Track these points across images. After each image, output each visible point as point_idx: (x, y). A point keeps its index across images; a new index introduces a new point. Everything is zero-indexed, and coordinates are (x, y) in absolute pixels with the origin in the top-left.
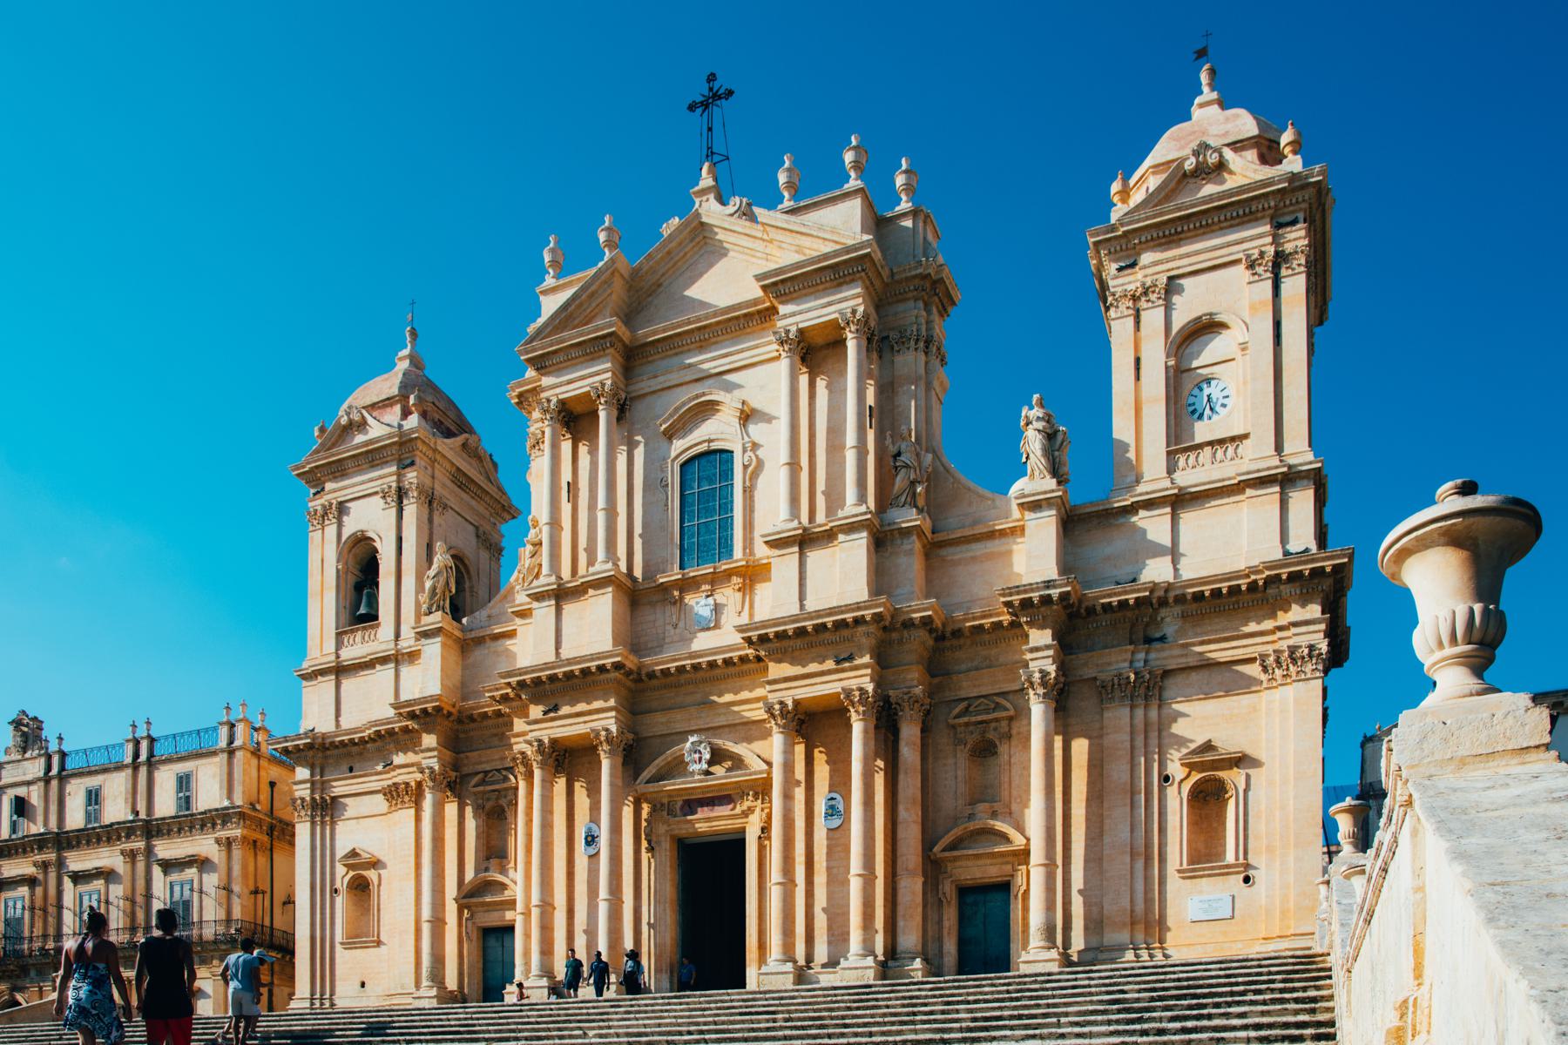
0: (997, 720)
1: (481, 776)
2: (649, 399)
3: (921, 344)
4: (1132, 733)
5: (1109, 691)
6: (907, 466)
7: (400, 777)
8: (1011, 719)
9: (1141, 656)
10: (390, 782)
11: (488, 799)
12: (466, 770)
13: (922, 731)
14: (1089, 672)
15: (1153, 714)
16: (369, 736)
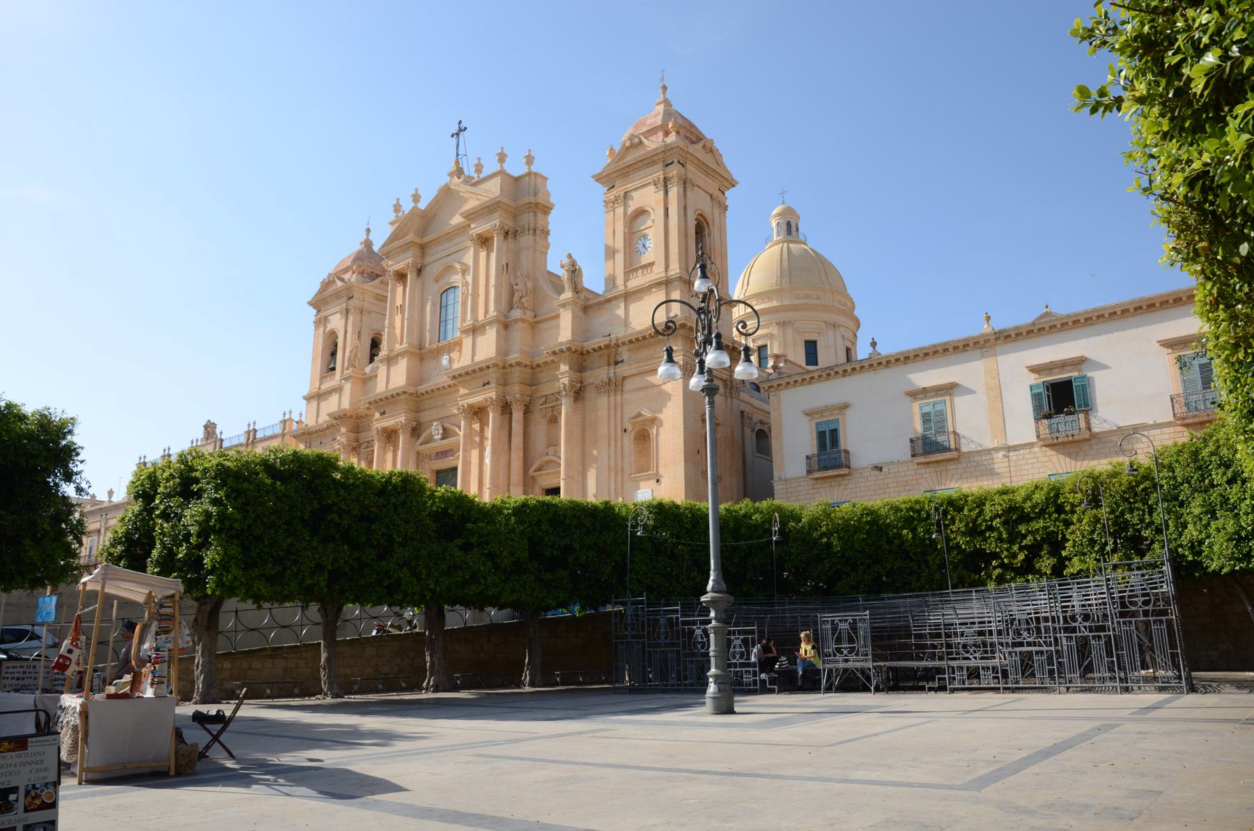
3: (531, 232)
4: (609, 409)
9: (612, 371)
12: (361, 441)
13: (524, 414)
14: (591, 381)
15: (619, 398)
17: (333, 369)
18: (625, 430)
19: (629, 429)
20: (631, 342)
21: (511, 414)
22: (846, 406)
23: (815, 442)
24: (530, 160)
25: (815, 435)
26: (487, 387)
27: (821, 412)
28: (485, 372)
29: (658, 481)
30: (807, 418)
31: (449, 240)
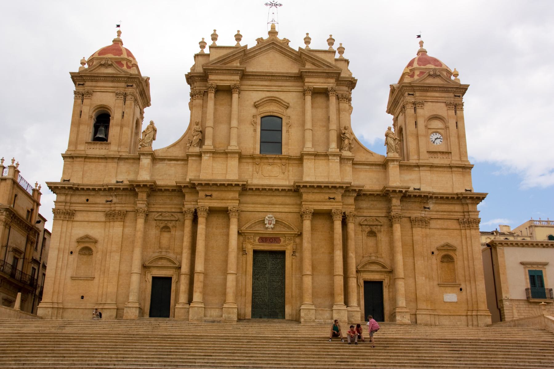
0: (377, 225)
1: (160, 213)
2: (247, 92)
3: (348, 100)
5: (413, 221)
6: (348, 138)
7: (118, 208)
8: (381, 225)
10: (113, 209)
11: (162, 223)
12: (152, 210)
16: (105, 188)
17: (104, 140)
18: (433, 253)
19: (436, 252)
20: (442, 198)
21: (332, 222)
22: (546, 264)
23: (528, 281)
24: (341, 50)
25: (528, 277)
26: (332, 200)
27: (532, 264)
28: (334, 191)
29: (461, 289)
30: (522, 266)
31: (271, 80)
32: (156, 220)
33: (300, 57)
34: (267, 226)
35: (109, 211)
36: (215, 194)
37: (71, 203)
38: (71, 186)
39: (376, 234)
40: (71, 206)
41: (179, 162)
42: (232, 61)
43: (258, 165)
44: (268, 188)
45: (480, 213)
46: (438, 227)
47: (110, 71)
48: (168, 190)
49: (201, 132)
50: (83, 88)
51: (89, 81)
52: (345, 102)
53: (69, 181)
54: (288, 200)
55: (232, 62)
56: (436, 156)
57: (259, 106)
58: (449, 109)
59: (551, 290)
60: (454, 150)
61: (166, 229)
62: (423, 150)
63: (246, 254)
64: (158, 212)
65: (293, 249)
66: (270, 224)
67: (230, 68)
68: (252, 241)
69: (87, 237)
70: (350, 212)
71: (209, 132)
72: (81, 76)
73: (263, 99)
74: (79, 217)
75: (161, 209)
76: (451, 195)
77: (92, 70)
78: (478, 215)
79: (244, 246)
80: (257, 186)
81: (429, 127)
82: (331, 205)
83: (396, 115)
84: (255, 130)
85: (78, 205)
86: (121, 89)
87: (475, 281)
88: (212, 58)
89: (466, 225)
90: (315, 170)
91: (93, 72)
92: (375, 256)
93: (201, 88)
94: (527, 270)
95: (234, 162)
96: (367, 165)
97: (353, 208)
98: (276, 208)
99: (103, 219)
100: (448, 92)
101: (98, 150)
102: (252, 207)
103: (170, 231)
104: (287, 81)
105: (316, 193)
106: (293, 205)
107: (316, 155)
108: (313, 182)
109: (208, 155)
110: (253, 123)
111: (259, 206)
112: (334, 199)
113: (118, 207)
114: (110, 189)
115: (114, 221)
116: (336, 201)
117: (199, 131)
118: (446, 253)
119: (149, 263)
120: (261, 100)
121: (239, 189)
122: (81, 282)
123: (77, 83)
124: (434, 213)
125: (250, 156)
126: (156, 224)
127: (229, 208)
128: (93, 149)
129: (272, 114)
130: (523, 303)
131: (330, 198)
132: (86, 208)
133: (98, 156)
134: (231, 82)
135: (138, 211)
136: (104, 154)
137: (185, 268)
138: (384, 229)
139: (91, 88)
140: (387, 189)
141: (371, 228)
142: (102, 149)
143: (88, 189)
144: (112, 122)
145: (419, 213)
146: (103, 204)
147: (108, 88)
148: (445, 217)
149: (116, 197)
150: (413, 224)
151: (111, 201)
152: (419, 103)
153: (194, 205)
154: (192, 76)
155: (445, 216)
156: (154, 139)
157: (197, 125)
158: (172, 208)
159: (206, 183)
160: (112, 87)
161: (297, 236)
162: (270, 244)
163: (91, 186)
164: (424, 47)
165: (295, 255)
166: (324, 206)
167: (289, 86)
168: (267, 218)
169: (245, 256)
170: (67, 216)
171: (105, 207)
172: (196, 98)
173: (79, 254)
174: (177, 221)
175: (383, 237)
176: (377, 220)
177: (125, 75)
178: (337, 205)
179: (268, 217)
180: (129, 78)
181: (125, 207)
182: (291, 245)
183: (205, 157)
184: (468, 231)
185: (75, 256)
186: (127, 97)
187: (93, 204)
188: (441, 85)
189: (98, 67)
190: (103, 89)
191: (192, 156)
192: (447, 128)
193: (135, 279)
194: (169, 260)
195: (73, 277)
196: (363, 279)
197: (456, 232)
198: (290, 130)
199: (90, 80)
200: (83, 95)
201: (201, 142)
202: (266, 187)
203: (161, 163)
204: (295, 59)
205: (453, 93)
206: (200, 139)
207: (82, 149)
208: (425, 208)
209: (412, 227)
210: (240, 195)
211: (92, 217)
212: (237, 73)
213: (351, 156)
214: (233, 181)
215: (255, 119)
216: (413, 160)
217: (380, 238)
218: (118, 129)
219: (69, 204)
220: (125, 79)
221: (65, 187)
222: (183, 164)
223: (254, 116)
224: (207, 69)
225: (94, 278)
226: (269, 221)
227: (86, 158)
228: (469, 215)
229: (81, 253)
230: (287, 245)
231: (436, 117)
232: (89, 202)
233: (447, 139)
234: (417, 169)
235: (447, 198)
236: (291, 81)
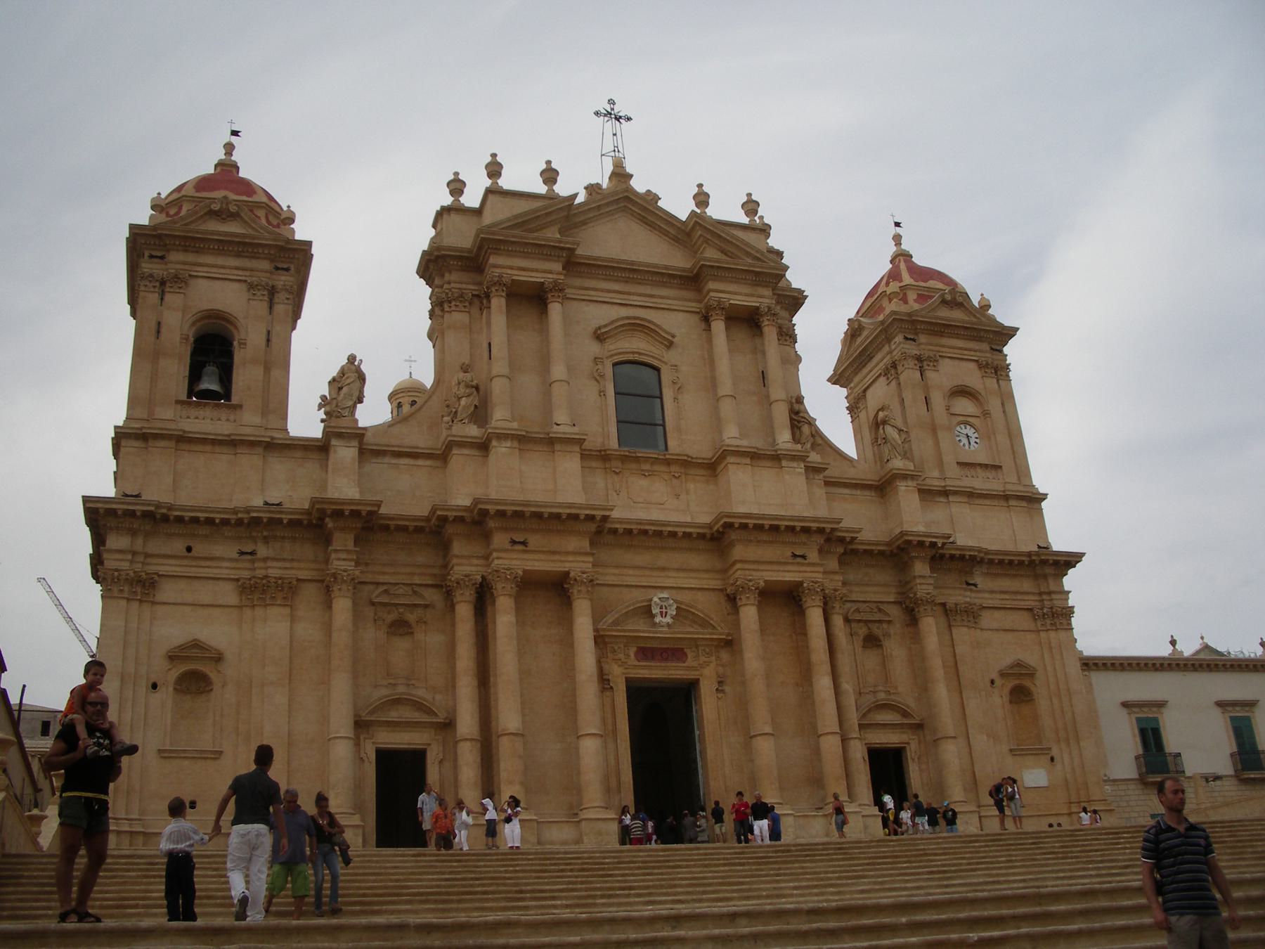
0: (880, 621)
2: (575, 304)
7: (275, 571)
8: (889, 622)
10: (260, 573)
11: (389, 613)
18: (992, 682)
19: (998, 682)
20: (1001, 562)
25: (1137, 732)
26: (799, 560)
28: (803, 538)
29: (1052, 759)
31: (627, 281)
32: (373, 604)
33: (689, 234)
34: (658, 619)
35: (250, 579)
36: (535, 540)
37: (147, 556)
38: (153, 508)
39: (880, 641)
40: (148, 564)
41: (420, 462)
42: (542, 228)
43: (617, 473)
44: (653, 528)
45: (1070, 595)
46: (995, 625)
47: (233, 228)
48: (404, 529)
49: (477, 388)
50: (163, 266)
51: (178, 251)
52: (788, 343)
53: (138, 496)
54: (696, 560)
55: (544, 228)
56: (973, 472)
57: (607, 338)
58: (984, 374)
59: (1179, 755)
60: (1007, 462)
61: (400, 627)
62: (949, 459)
63: (612, 688)
64: (378, 584)
65: (719, 677)
66: (663, 615)
67: (543, 243)
68: (621, 656)
69: (196, 645)
70: (835, 590)
71: (498, 389)
72: (160, 237)
73: (617, 320)
74: (168, 591)
75: (387, 577)
76: (1019, 555)
77: (186, 224)
78: (1067, 599)
79: (606, 667)
80: (628, 523)
81: (953, 410)
82: (800, 572)
83: (858, 390)
84: (602, 393)
85: (166, 561)
86: (259, 274)
87: (1078, 740)
88: (488, 218)
89: (1048, 622)
90: (755, 491)
91: (192, 226)
92: (885, 692)
93: (464, 286)
94: (1134, 716)
95: (570, 465)
96: (846, 485)
97: (838, 581)
98: (670, 577)
99: (233, 599)
100: (978, 339)
101: (206, 421)
102: (614, 574)
103: (412, 633)
104: (662, 284)
105: (765, 542)
106: (707, 571)
107: (754, 456)
108: (763, 517)
109: (509, 444)
110: (595, 375)
111: (631, 572)
112: (804, 557)
113: (273, 567)
114: (256, 522)
115: (266, 606)
116: (806, 562)
117: (472, 387)
118: (1017, 682)
119: (367, 714)
120: (612, 322)
121: (592, 527)
122: (186, 763)
123: (147, 254)
124: (987, 595)
125: (598, 453)
126: (376, 614)
127: (572, 574)
128: (197, 418)
129: (636, 357)
130: (1133, 787)
131: (795, 556)
132: (188, 569)
133: (213, 437)
134: (545, 275)
135: (335, 578)
136: (226, 433)
137: (467, 723)
138: (896, 629)
139: (182, 267)
140: (906, 538)
141: (869, 629)
142: (220, 419)
143: (195, 520)
144: (238, 356)
145: (960, 595)
146: (231, 560)
147: (228, 271)
148: (1009, 604)
149: (267, 543)
150: (951, 619)
151: (252, 553)
152: (929, 359)
153: (477, 565)
154: (444, 257)
155: (1008, 602)
156: (360, 400)
157: (465, 372)
158: (412, 574)
159: (516, 512)
160: (237, 268)
161: (722, 644)
162: (663, 665)
163: (202, 511)
164: (903, 247)
165: (723, 691)
166: (787, 574)
167: (668, 298)
168: (656, 599)
169: (608, 693)
170: (139, 590)
171: (238, 569)
172: (453, 308)
173: (175, 689)
174: (426, 606)
175: (896, 649)
176: (880, 610)
177: (275, 240)
178: (812, 572)
179: (660, 598)
180: (282, 249)
181: (292, 568)
182: (713, 665)
183: (501, 450)
184: (1052, 634)
185: (166, 695)
186: (276, 295)
187: (206, 559)
188: (968, 323)
189: (202, 216)
190: (215, 272)
191: (461, 444)
192: (986, 414)
193: (342, 751)
194: (419, 706)
195: (165, 751)
196: (866, 744)
197: (1029, 636)
198: (680, 397)
199: (180, 248)
200: (163, 283)
201: (480, 414)
202: (647, 527)
203: (374, 460)
204: (676, 240)
205: (989, 343)
206: (475, 406)
207: (170, 416)
208: (968, 584)
209: (950, 627)
210: (592, 544)
211: (205, 592)
212: (559, 257)
213: (819, 463)
214: (580, 508)
215: (600, 366)
216: (933, 478)
217: (889, 650)
218: (259, 371)
219: (141, 558)
220: (272, 252)
221: (134, 511)
222: (431, 466)
223: (596, 360)
224: (489, 239)
225: (222, 752)
226: (661, 608)
227: (183, 440)
228: (1051, 600)
229: (178, 687)
230: (701, 666)
231: (962, 392)
232: (194, 553)
233: (989, 438)
234: (942, 499)
235: (1011, 563)
236: (671, 287)
